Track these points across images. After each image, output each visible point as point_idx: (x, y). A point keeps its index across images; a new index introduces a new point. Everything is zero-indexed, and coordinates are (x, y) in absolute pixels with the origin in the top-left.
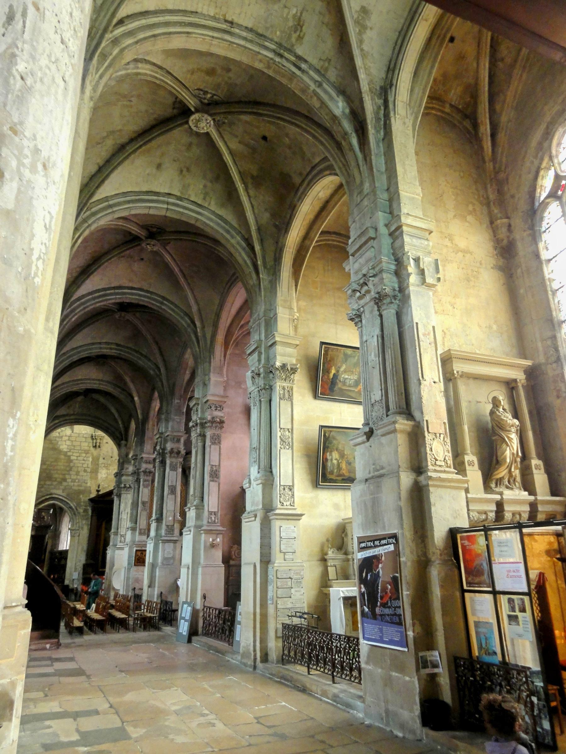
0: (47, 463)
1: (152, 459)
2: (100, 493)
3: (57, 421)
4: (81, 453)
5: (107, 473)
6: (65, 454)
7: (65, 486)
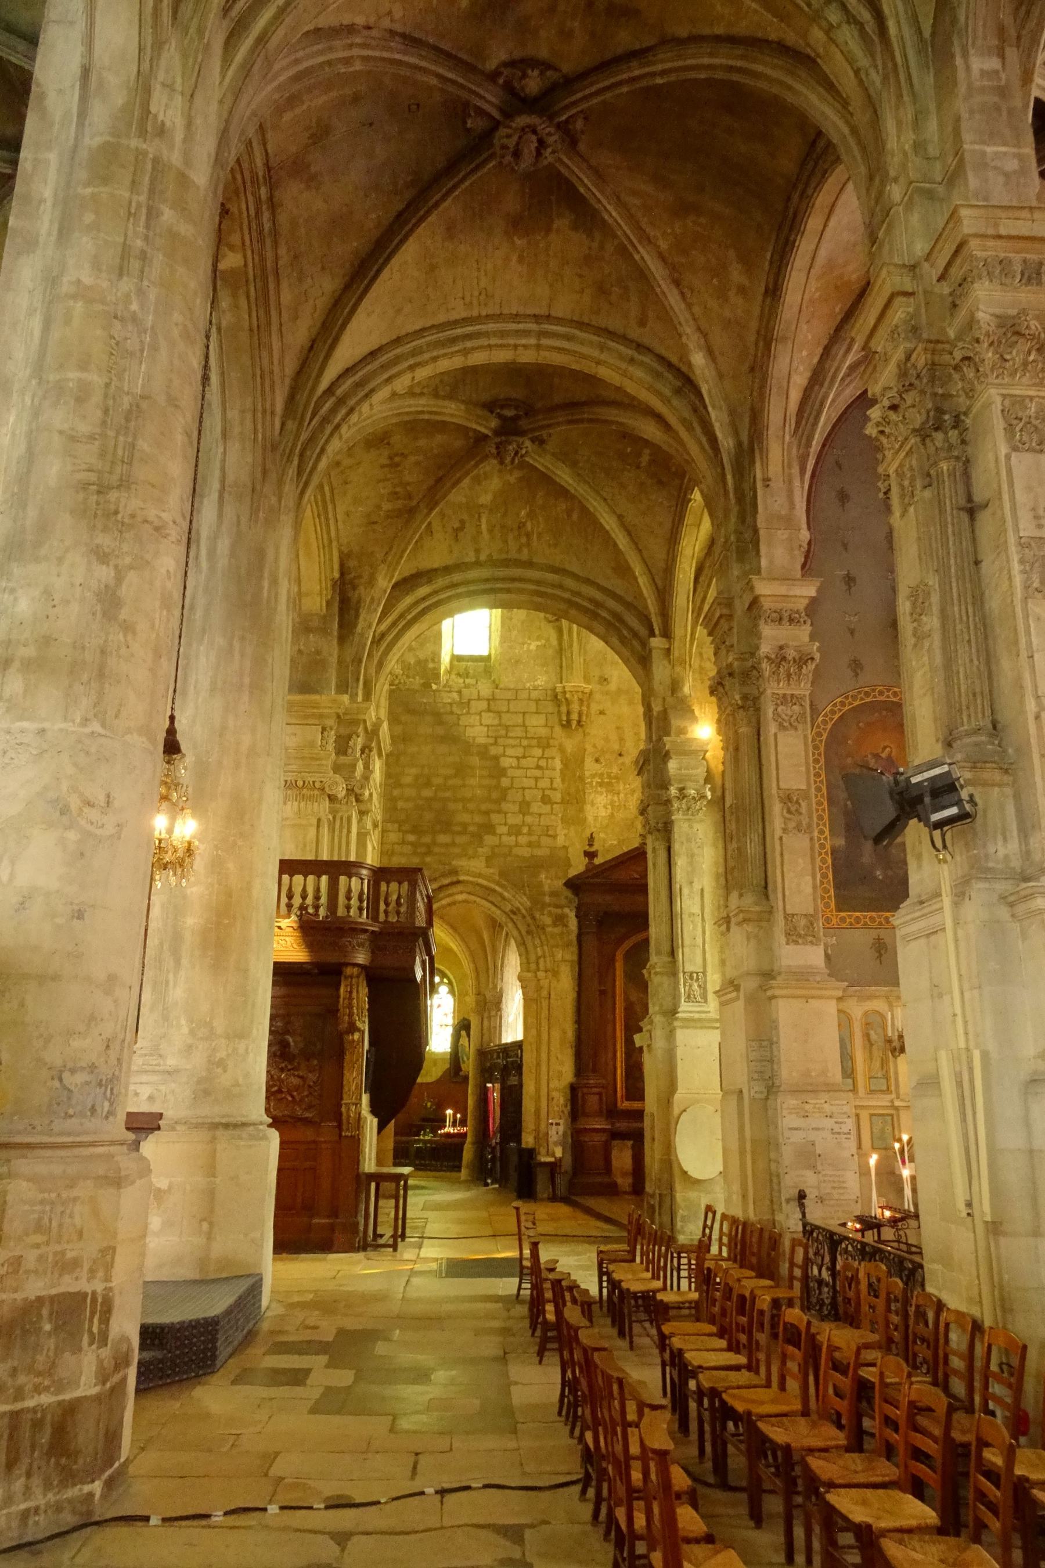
0: (437, 781)
1: (801, 605)
2: (597, 861)
3: (423, 591)
4: (529, 746)
5: (612, 803)
6: (483, 752)
7: (493, 848)
